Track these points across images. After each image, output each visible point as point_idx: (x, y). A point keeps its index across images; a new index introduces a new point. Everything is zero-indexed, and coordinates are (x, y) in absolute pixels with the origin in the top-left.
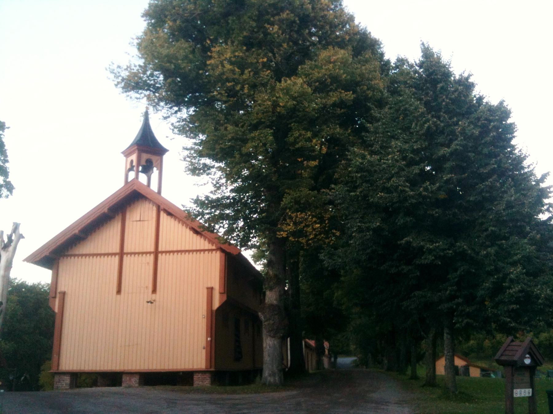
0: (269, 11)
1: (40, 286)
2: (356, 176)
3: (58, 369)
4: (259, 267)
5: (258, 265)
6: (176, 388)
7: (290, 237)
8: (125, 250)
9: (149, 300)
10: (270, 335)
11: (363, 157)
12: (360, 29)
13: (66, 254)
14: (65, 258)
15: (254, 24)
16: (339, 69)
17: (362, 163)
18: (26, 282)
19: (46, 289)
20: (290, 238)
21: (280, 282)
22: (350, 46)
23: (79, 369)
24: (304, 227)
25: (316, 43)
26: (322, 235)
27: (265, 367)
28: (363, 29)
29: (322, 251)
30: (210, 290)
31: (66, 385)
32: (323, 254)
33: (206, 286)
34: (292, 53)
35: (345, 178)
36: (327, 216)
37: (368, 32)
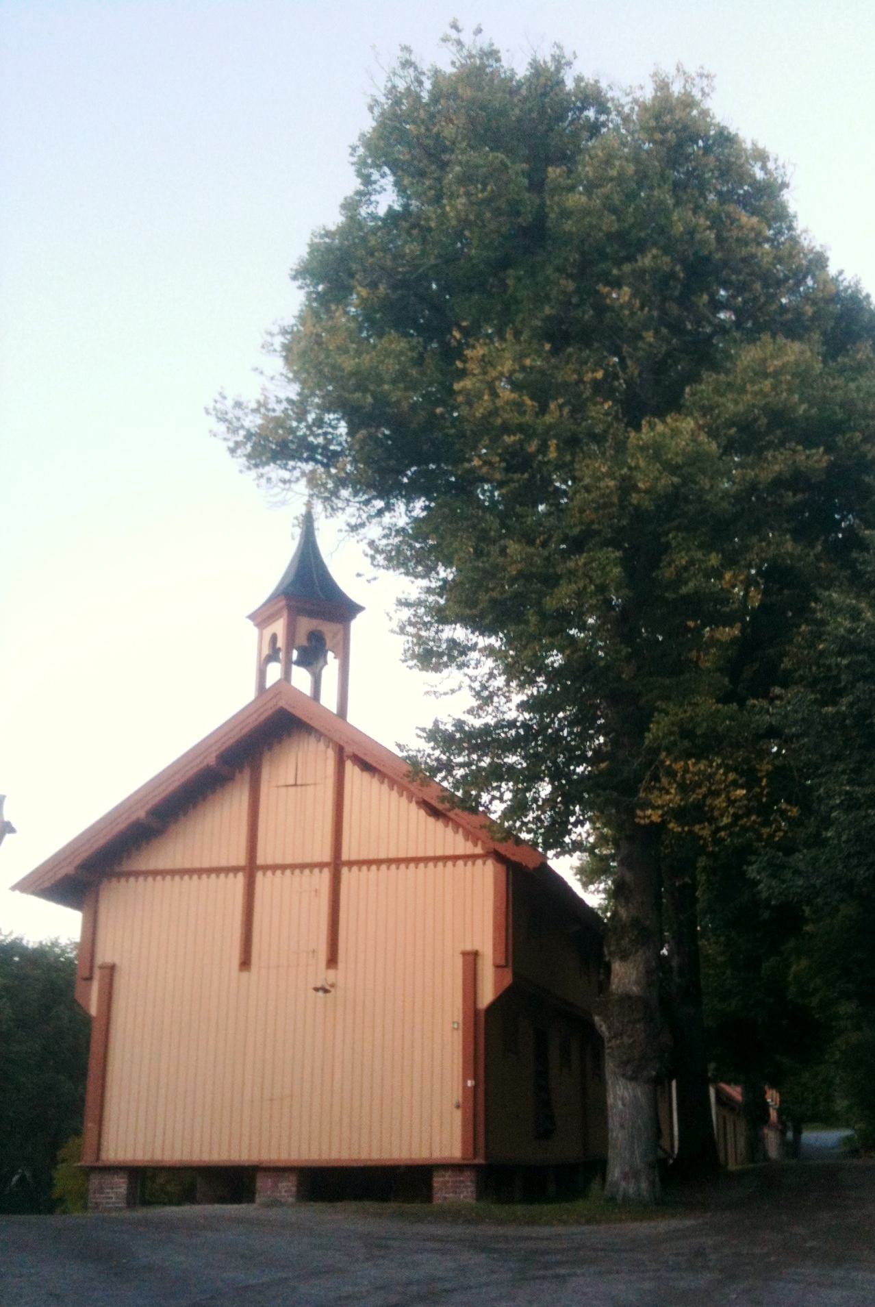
0: (608, 250)
1: (57, 950)
2: (837, 665)
3: (98, 1159)
4: (594, 897)
5: (593, 893)
6: (392, 1206)
7: (670, 821)
8: (260, 861)
9: (319, 985)
10: (623, 1075)
11: (856, 615)
12: (841, 288)
13: (117, 869)
14: (114, 880)
15: (571, 286)
16: (790, 391)
17: (851, 631)
18: (21, 939)
19: (72, 955)
20: (671, 825)
21: (647, 936)
22: (818, 332)
23: (148, 1157)
24: (705, 797)
25: (728, 326)
26: (753, 818)
27: (611, 1154)
28: (849, 287)
29: (753, 858)
30: (472, 959)
31: (117, 1198)
32: (755, 866)
34: (668, 355)
35: (810, 669)
36: (766, 767)
37: (864, 294)
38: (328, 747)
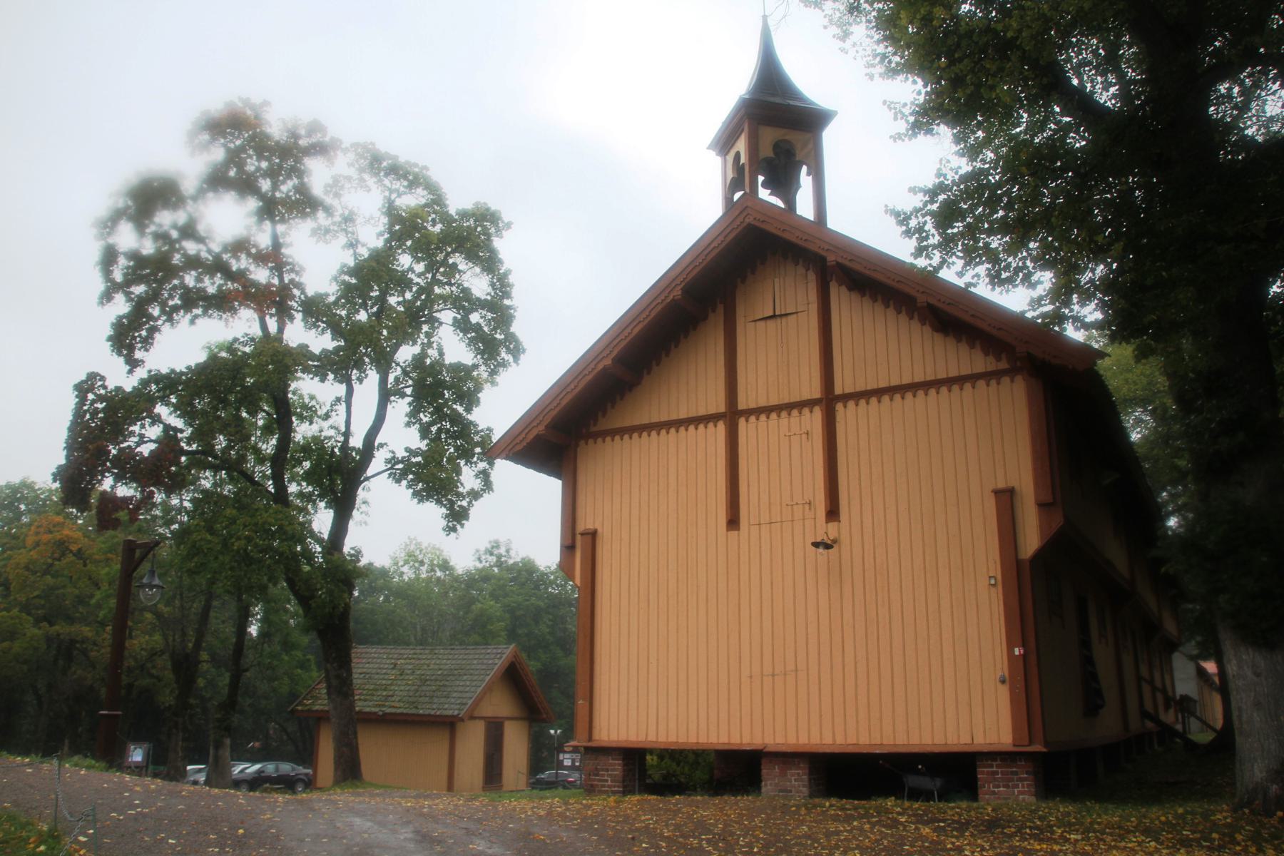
3: (590, 739)
8: (742, 405)
9: (819, 540)
13: (593, 429)
23: (642, 738)
30: (1006, 498)
31: (612, 782)
33: (992, 487)
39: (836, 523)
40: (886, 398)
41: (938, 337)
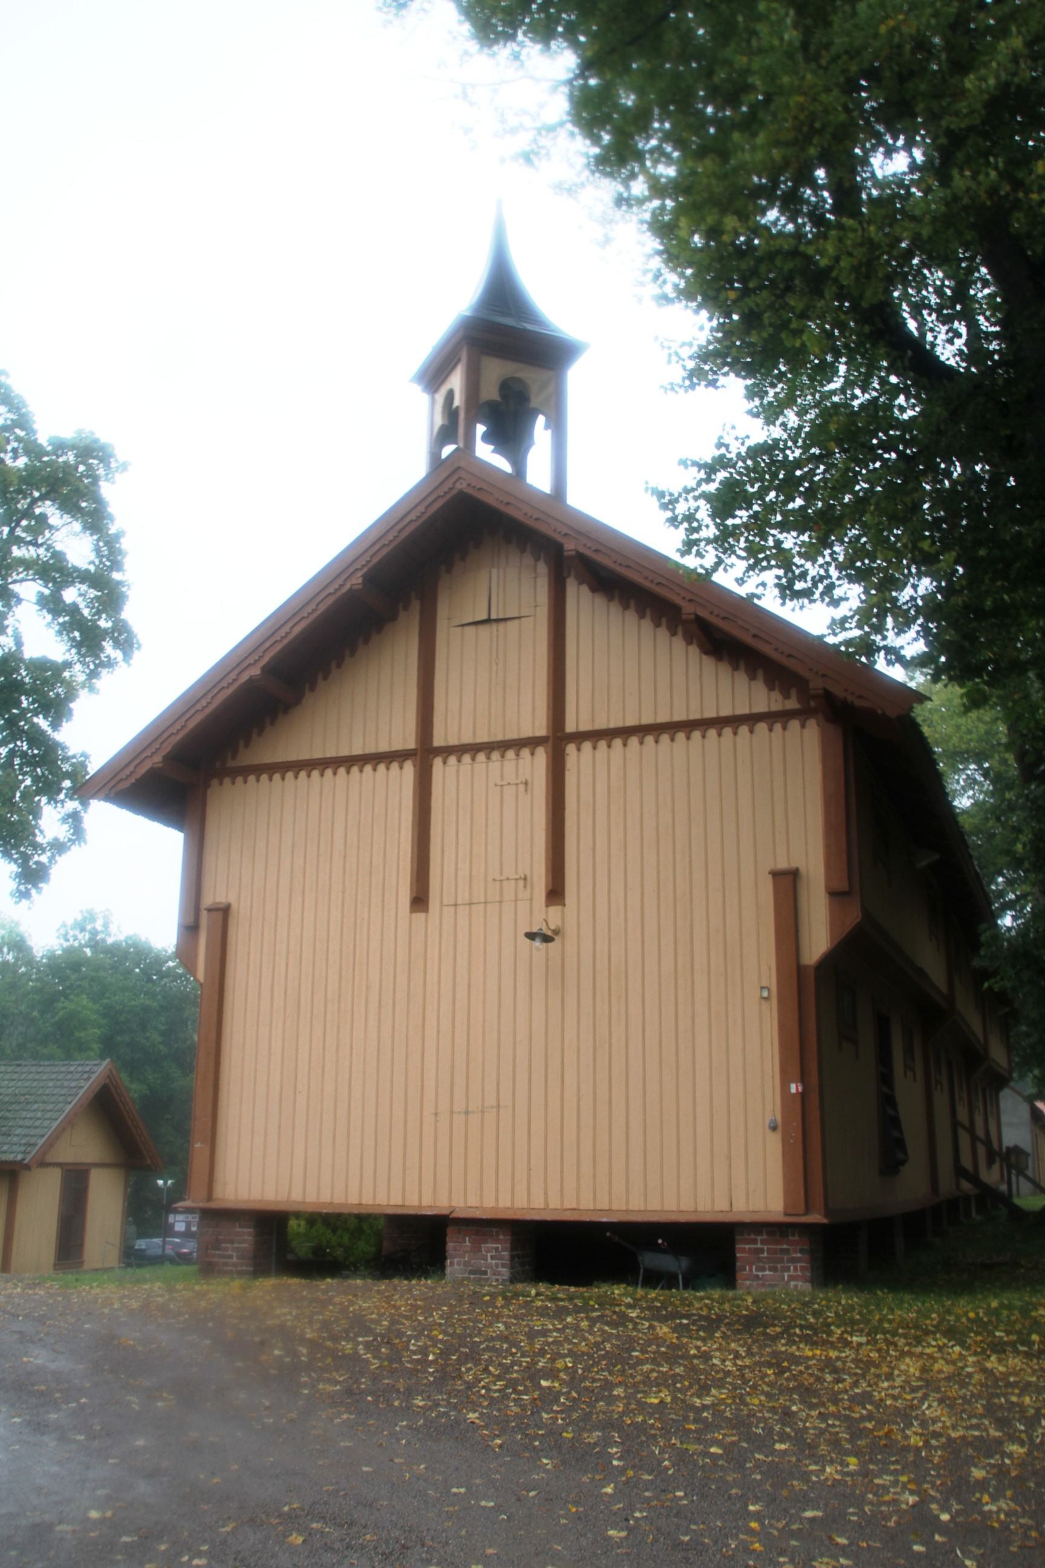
3: (210, 1197)
8: (438, 741)
9: (535, 930)
13: (231, 764)
14: (227, 781)
23: (282, 1196)
31: (237, 1257)
33: (770, 865)
38: (537, 559)
39: (560, 908)
40: (634, 741)
41: (709, 662)
